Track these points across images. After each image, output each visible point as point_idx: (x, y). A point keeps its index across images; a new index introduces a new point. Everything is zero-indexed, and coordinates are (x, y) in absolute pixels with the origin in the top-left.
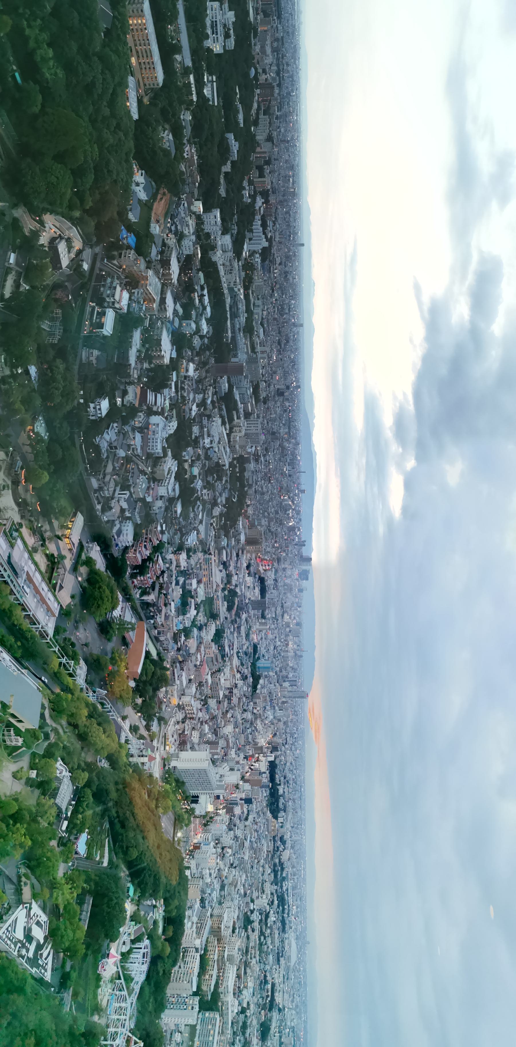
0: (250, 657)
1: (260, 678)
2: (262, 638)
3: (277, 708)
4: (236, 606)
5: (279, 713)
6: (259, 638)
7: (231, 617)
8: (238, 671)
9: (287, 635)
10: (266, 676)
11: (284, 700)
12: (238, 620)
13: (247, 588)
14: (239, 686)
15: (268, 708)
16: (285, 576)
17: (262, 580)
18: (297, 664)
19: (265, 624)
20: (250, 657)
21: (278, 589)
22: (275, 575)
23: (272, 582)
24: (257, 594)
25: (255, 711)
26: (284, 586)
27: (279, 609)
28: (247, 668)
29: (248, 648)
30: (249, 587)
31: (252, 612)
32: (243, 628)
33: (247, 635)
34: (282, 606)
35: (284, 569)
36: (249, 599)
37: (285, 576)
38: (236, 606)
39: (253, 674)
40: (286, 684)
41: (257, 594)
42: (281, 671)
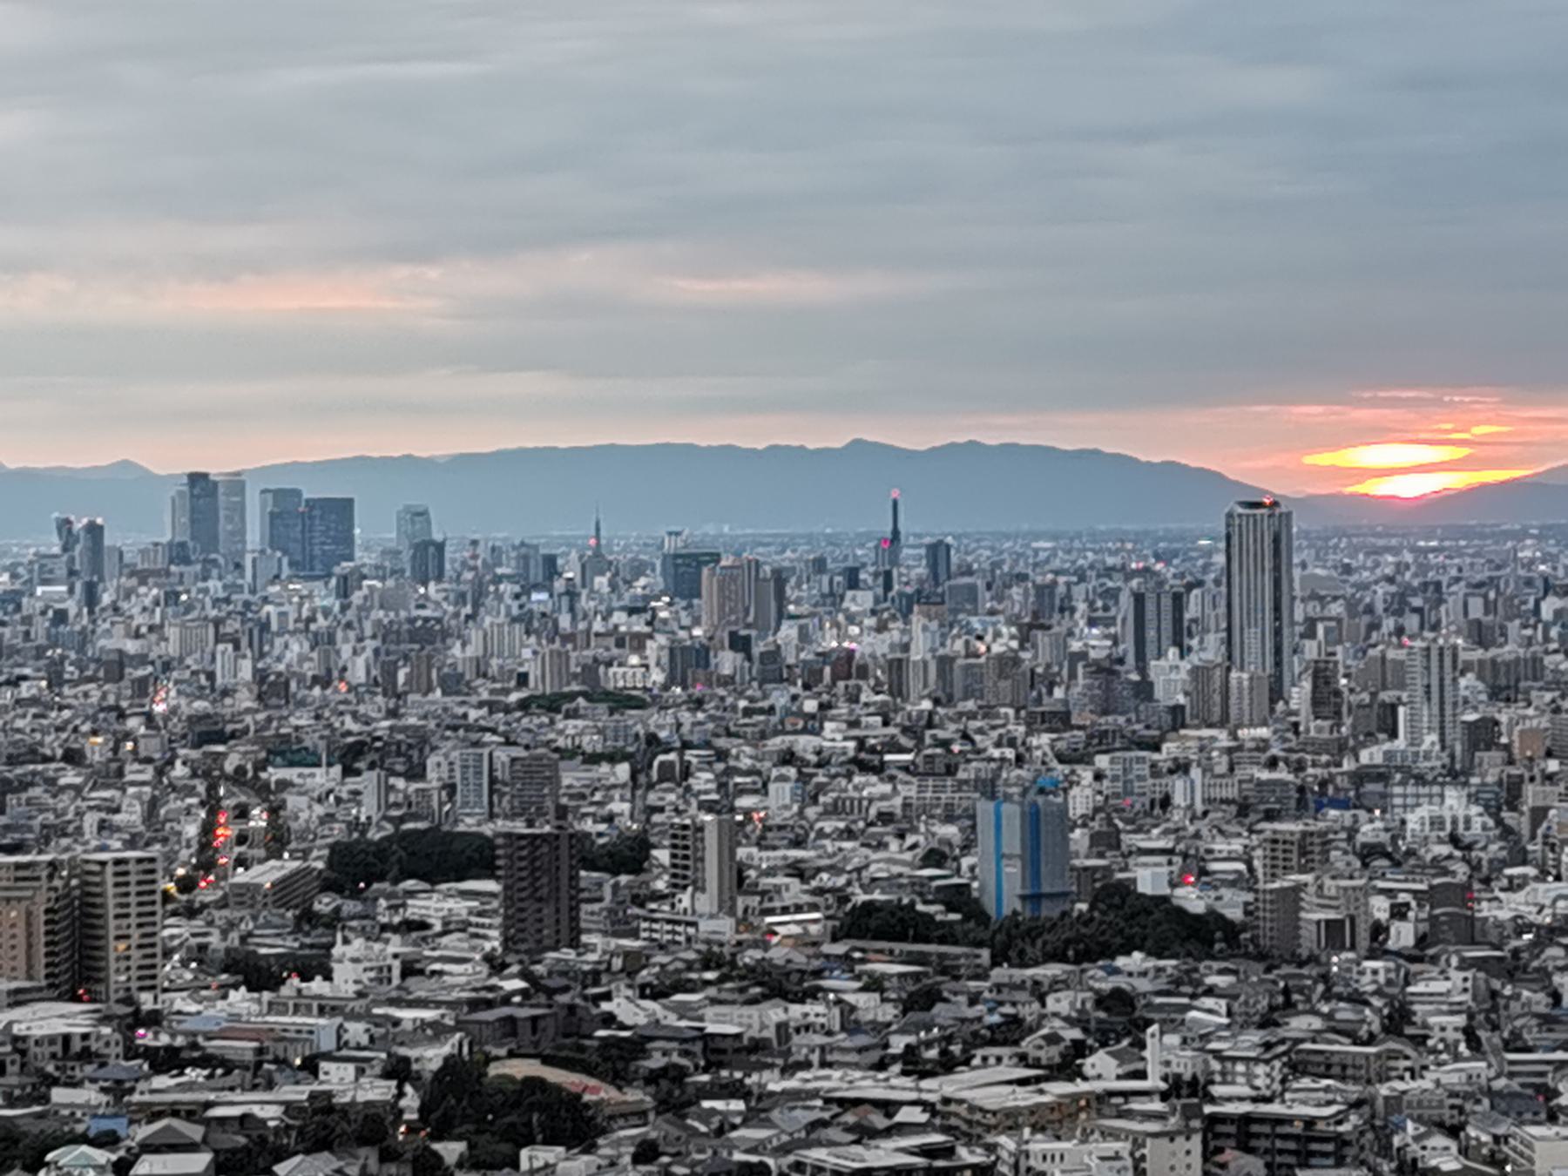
0: (948, 970)
1: (1126, 890)
2: (799, 871)
3: (1371, 755)
4: (554, 1075)
5: (1419, 737)
6: (795, 890)
7: (641, 1115)
8: (1067, 1068)
9: (773, 669)
10: (1106, 841)
11: (1299, 695)
12: (656, 1062)
13: (419, 987)
14: (1185, 1063)
15: (1371, 830)
16: (324, 681)
17: (358, 867)
18: (998, 585)
19: (686, 840)
20: (948, 970)
21: (422, 741)
22: (309, 759)
23: (368, 781)
24: (461, 907)
25: (1403, 935)
26: (391, 690)
27: (568, 730)
28: (1039, 992)
29: (875, 984)
30: (409, 970)
31: (598, 945)
32: (723, 1022)
33: (778, 985)
34: (553, 704)
35: (272, 689)
36: (496, 965)
37: (324, 681)
38: (554, 1075)
39: (1090, 947)
40: (1170, 676)
41: (461, 907)
42: (1060, 720)
